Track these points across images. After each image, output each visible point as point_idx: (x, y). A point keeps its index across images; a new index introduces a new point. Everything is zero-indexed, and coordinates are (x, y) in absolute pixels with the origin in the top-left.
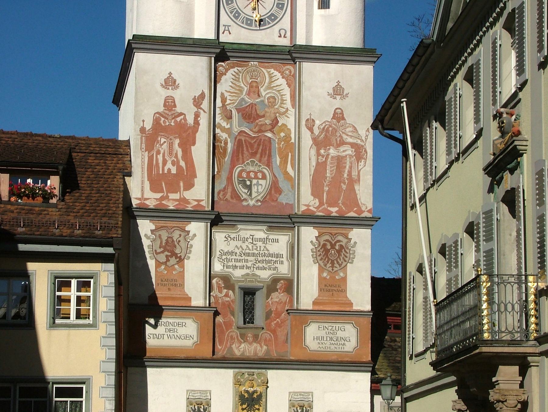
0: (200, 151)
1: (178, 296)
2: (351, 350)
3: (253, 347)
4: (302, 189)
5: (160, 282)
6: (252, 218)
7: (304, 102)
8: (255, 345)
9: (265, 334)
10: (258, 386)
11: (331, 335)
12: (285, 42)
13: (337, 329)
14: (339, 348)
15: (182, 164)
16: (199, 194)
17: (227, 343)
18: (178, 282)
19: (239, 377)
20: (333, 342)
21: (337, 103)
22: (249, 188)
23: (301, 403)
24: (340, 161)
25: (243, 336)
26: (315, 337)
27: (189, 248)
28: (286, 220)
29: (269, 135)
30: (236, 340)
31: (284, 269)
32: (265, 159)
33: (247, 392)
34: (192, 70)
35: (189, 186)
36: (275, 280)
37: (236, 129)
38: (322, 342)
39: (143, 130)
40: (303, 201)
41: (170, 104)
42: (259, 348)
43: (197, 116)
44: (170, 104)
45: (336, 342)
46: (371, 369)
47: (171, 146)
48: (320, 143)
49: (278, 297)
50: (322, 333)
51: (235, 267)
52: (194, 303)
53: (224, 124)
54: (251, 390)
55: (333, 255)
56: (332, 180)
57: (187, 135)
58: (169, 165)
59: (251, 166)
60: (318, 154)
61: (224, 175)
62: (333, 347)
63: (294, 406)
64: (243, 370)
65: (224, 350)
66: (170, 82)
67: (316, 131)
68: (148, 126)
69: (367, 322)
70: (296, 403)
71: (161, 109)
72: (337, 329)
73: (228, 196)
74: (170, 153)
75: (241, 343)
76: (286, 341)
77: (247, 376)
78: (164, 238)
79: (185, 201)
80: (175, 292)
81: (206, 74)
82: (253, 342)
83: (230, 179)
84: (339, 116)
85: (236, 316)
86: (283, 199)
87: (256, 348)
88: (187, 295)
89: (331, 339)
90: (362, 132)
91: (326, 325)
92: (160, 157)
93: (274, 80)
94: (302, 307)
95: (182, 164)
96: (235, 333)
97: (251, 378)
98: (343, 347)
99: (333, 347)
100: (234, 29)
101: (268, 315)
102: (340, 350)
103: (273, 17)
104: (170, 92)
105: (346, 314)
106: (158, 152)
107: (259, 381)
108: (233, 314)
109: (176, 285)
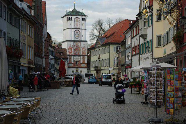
6: (77, 56)
16: (73, 53)
26: (82, 65)
28: (80, 56)
31: (80, 60)
34: (72, 43)
41: (70, 46)
44: (70, 46)
55: (84, 58)
56: (84, 52)
57: (72, 49)
59: (77, 51)
66: (70, 44)
93: (79, 43)
105: (85, 63)
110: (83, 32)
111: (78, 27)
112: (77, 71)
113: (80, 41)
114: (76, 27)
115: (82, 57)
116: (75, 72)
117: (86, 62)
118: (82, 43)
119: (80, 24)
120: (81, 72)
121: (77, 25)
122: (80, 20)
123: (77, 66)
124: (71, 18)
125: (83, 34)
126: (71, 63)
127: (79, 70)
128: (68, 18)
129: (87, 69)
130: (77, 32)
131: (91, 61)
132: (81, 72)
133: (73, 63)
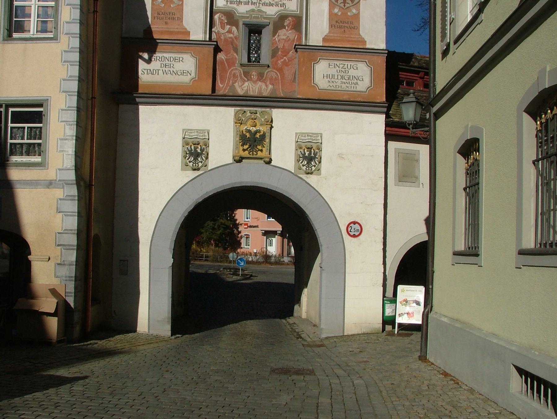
1: (176, 30)
2: (364, 90)
3: (258, 86)
5: (156, 15)
8: (260, 83)
9: (271, 73)
10: (261, 125)
11: (342, 74)
13: (349, 67)
14: (351, 88)
17: (229, 81)
18: (176, 15)
19: (240, 115)
20: (345, 81)
23: (309, 145)
26: (325, 75)
30: (239, 78)
33: (249, 131)
38: (333, 80)
42: (264, 87)
45: (347, 81)
46: (385, 110)
50: (333, 71)
54: (253, 129)
62: (344, 86)
63: (301, 148)
64: (245, 109)
65: (225, 89)
69: (381, 61)
70: (303, 145)
72: (349, 67)
75: (244, 81)
77: (249, 114)
80: (173, 26)
82: (257, 80)
85: (240, 53)
87: (260, 88)
88: (186, 29)
89: (342, 77)
91: (338, 63)
96: (239, 71)
97: (253, 116)
98: (355, 86)
99: (344, 86)
101: (274, 53)
102: (352, 89)
105: (360, 51)
107: (263, 120)
108: (236, 50)
109: (173, 19)
112: (253, 143)
120: (310, 156)
123: (244, 87)
129: (395, 131)
132: (310, 156)
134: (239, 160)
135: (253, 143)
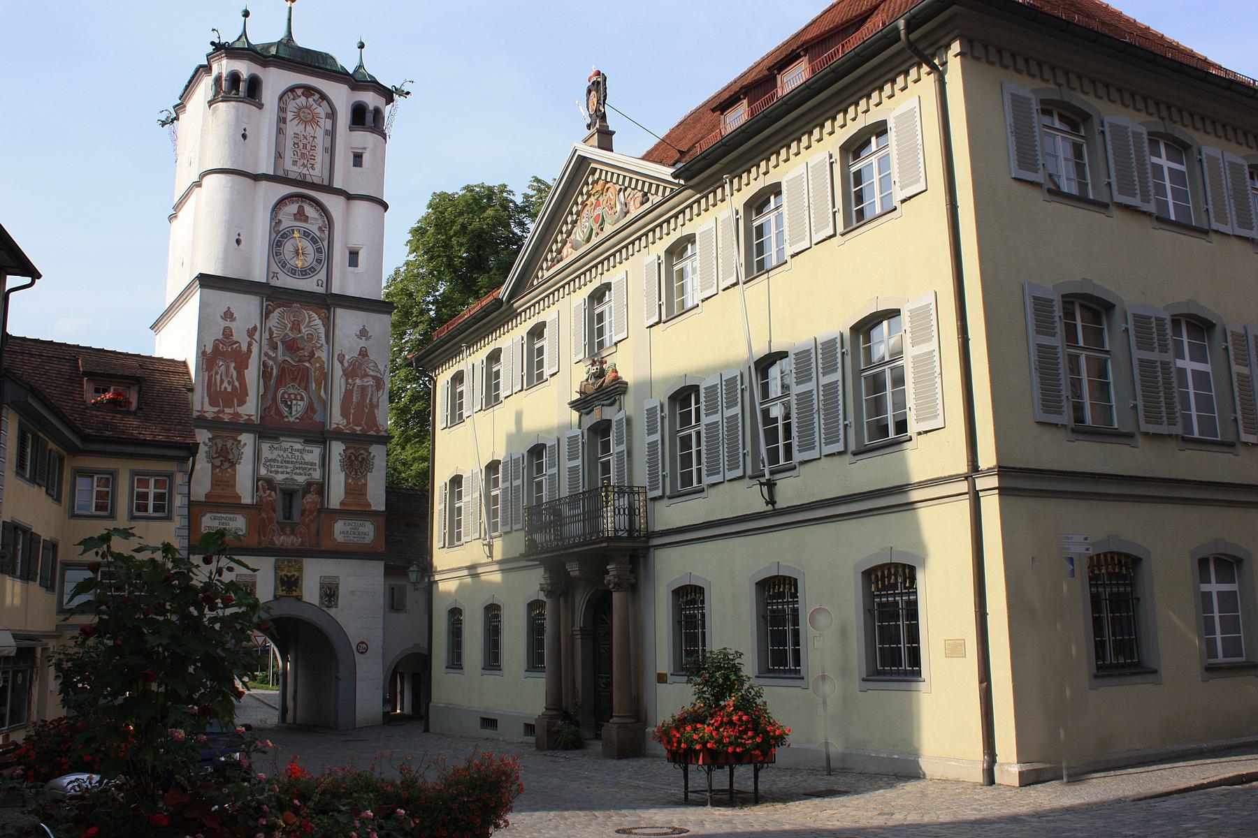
0: (252, 374)
4: (334, 410)
6: (292, 432)
7: (337, 340)
12: (322, 290)
15: (237, 384)
16: (250, 409)
21: (363, 343)
22: (290, 407)
24: (363, 389)
25: (283, 530)
26: (341, 530)
27: (240, 455)
28: (319, 435)
29: (307, 364)
31: (317, 475)
32: (303, 384)
35: (242, 402)
36: (309, 484)
37: (280, 359)
39: (204, 353)
40: (334, 420)
41: (227, 333)
43: (250, 345)
44: (227, 333)
47: (227, 368)
48: (348, 374)
49: (312, 498)
50: (347, 528)
51: (277, 472)
52: (244, 501)
53: (271, 353)
55: (356, 466)
56: (360, 406)
57: (241, 360)
58: (225, 384)
60: (347, 383)
61: (270, 395)
66: (228, 315)
67: (346, 364)
68: (209, 350)
71: (220, 337)
73: (272, 413)
74: (227, 375)
76: (318, 534)
78: (220, 446)
79: (237, 415)
81: (258, 311)
83: (274, 398)
84: (363, 353)
86: (317, 418)
90: (381, 368)
92: (218, 377)
93: (313, 321)
94: (331, 507)
95: (237, 384)
100: (282, 276)
101: (303, 512)
103: (313, 270)
104: (228, 324)
106: (217, 373)
110: (351, 224)
111: (317, 173)
112: (289, 584)
113: (328, 302)
114: (294, 171)
115: (337, 448)
116: (265, 591)
117: (377, 497)
118: (348, 322)
119: (331, 151)
120: (330, 593)
121: (304, 152)
122: (332, 115)
123: (282, 540)
124: (254, 85)
125: (354, 242)
126: (235, 506)
127: (314, 573)
128: (218, 80)
129: (389, 572)
130: (301, 216)
131: (441, 478)
132: (330, 593)
133: (247, 499)
134: (276, 598)
135: (289, 584)
